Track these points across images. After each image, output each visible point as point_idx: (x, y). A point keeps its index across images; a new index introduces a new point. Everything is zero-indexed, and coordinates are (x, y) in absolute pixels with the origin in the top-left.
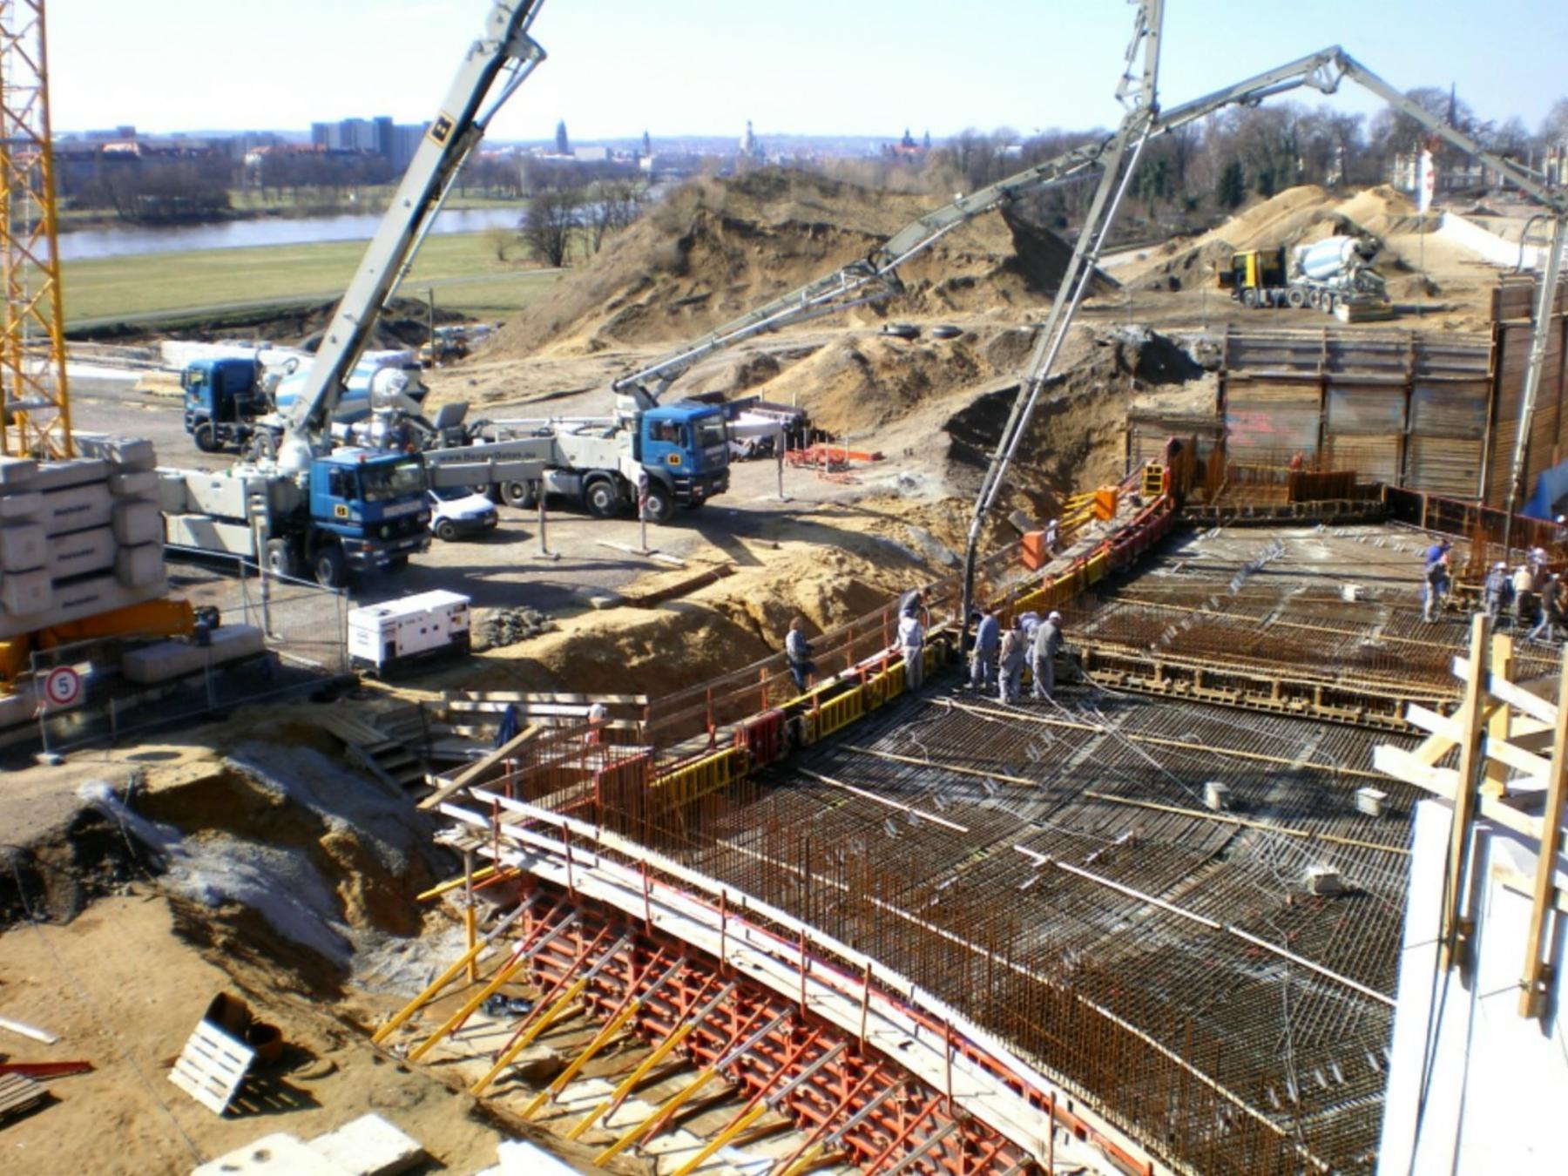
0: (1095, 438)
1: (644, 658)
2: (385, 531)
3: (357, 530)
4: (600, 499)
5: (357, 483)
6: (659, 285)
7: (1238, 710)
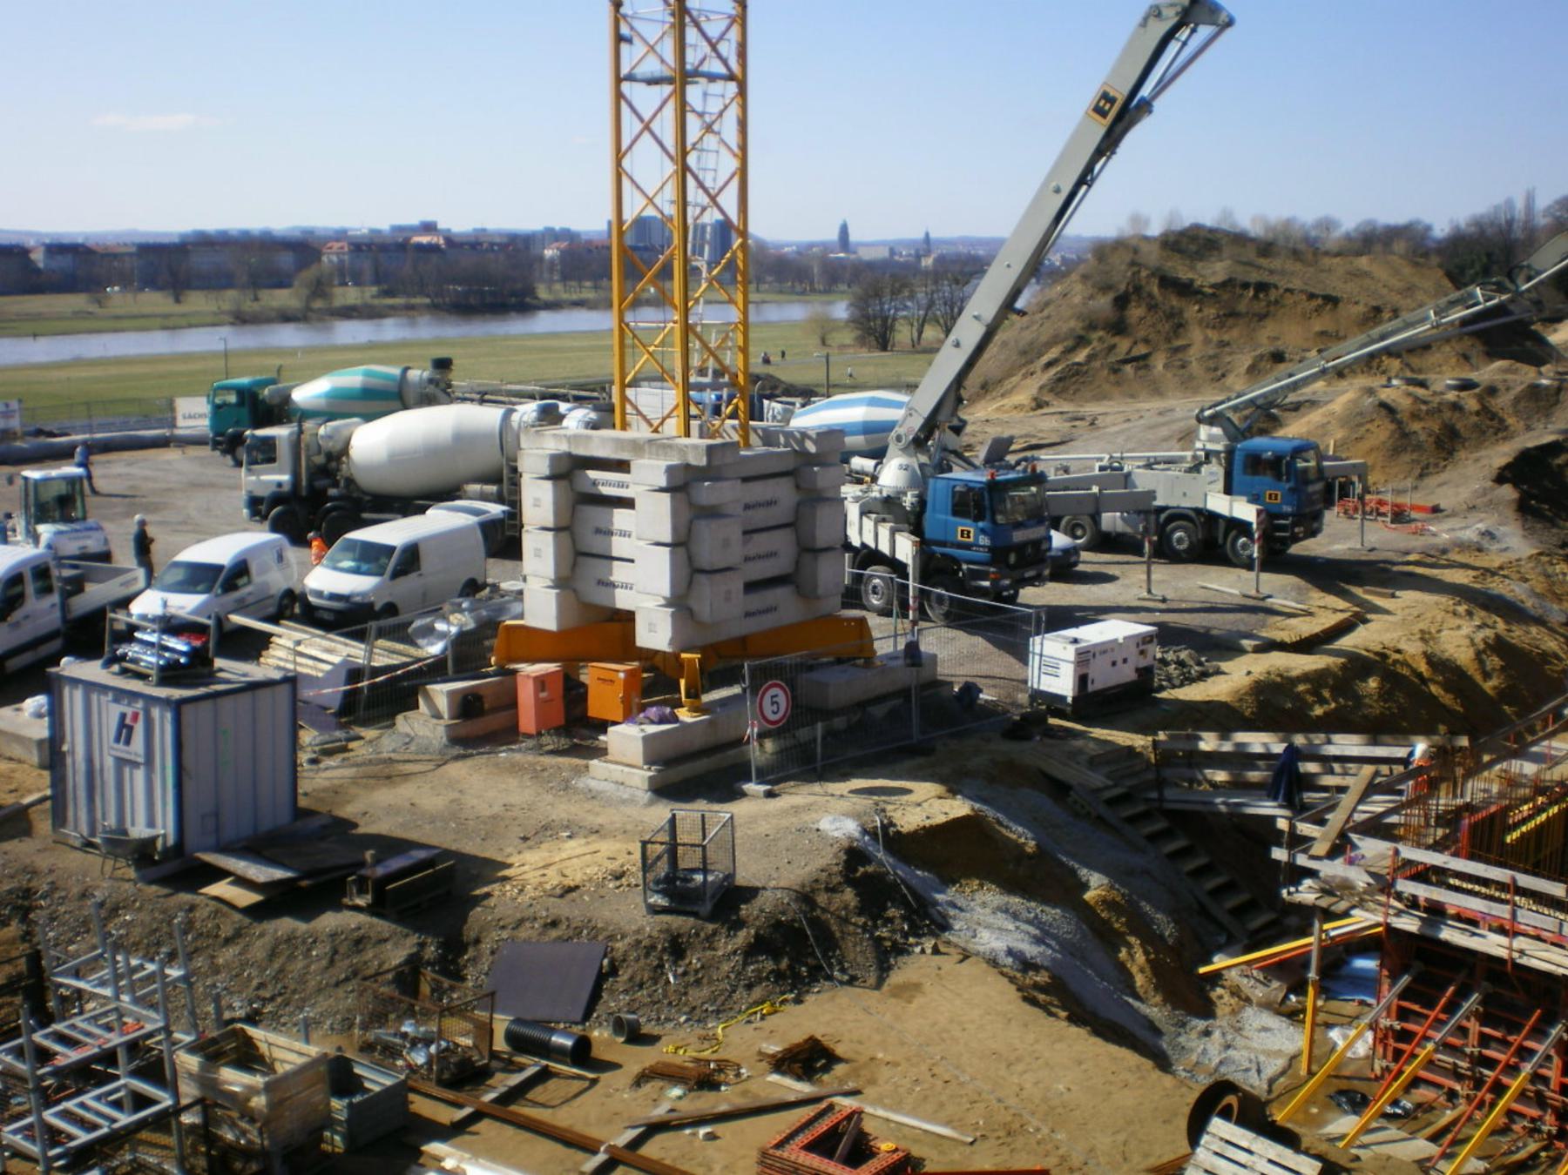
1: (1326, 707)
2: (1012, 558)
3: (983, 555)
4: (1180, 540)
5: (987, 503)
6: (1095, 344)
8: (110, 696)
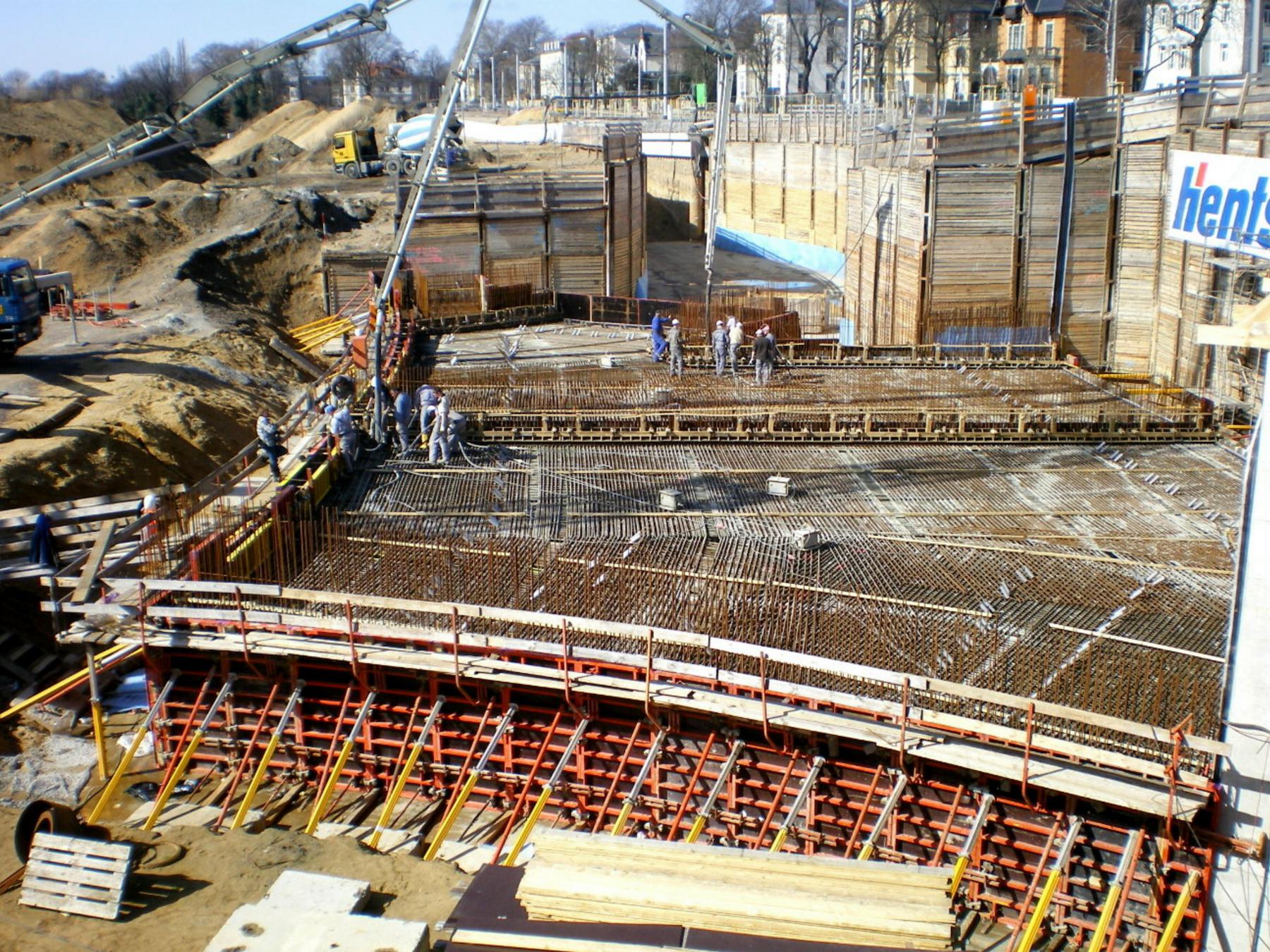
0: (294, 280)
7: (616, 443)
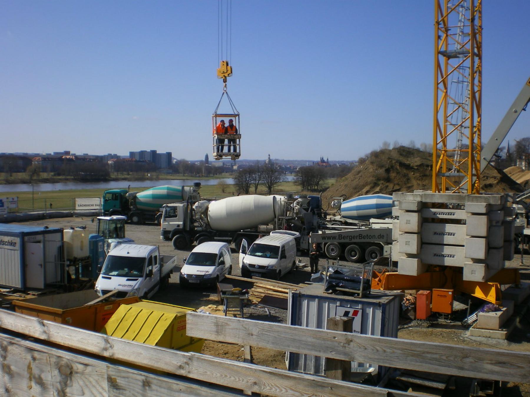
8: (338, 303)
